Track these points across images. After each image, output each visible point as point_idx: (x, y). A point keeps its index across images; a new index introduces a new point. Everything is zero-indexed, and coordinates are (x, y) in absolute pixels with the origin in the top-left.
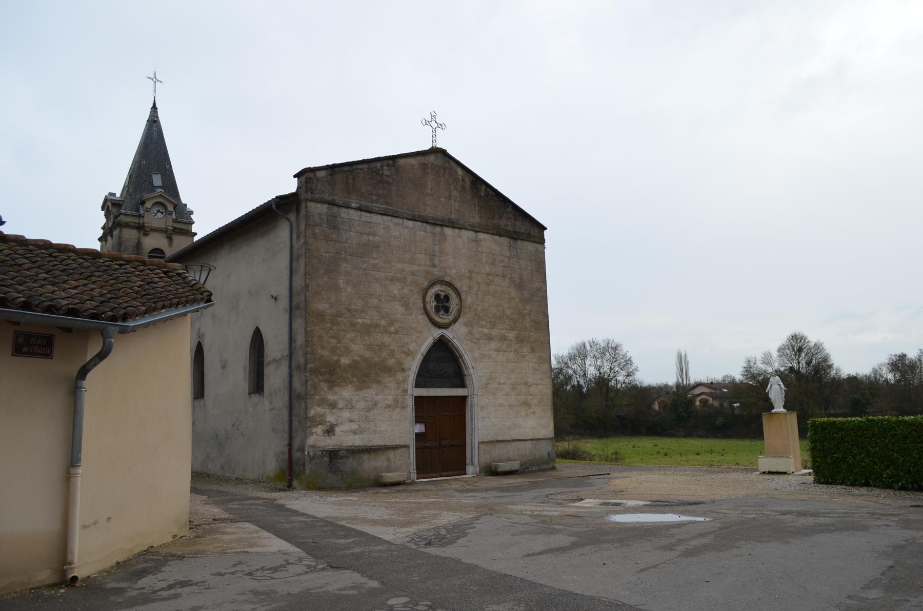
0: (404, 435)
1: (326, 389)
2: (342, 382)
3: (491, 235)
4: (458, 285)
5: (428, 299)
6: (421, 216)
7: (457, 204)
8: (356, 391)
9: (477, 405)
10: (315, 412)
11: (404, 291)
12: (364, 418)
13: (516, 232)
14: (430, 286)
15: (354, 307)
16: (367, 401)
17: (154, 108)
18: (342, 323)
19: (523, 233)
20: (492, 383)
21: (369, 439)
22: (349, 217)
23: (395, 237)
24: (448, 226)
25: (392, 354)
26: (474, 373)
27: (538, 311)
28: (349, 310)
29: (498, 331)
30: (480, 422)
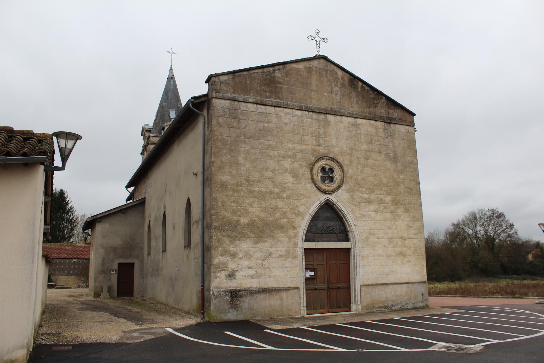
0: (295, 279)
1: (228, 242)
2: (241, 237)
3: (368, 121)
4: (340, 159)
5: (315, 171)
6: (307, 107)
7: (338, 97)
8: (254, 244)
9: (359, 255)
10: (219, 261)
12: (261, 266)
13: (390, 118)
14: (316, 161)
16: (263, 252)
17: (171, 70)
18: (242, 191)
19: (396, 118)
20: (371, 237)
21: (265, 282)
22: (247, 109)
23: (286, 124)
24: (331, 114)
25: (284, 215)
26: (356, 230)
28: (248, 181)
29: (376, 196)
30: (361, 269)
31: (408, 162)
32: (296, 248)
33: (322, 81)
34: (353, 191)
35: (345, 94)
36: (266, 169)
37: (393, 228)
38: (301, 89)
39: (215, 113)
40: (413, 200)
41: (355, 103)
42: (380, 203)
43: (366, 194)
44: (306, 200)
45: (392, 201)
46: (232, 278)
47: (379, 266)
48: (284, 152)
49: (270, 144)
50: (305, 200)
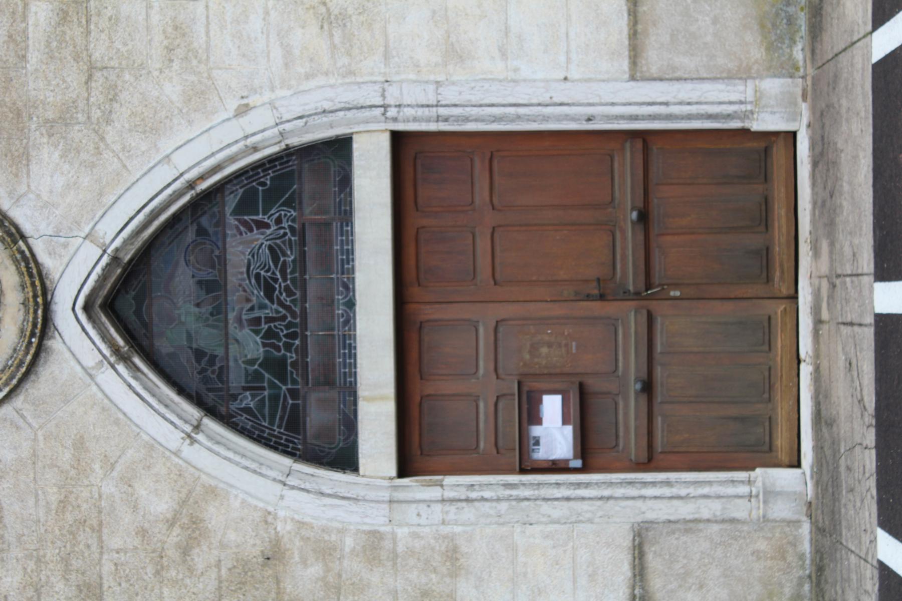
9: (438, 83)
26: (272, 105)
34: (19, 115)
44: (97, 466)
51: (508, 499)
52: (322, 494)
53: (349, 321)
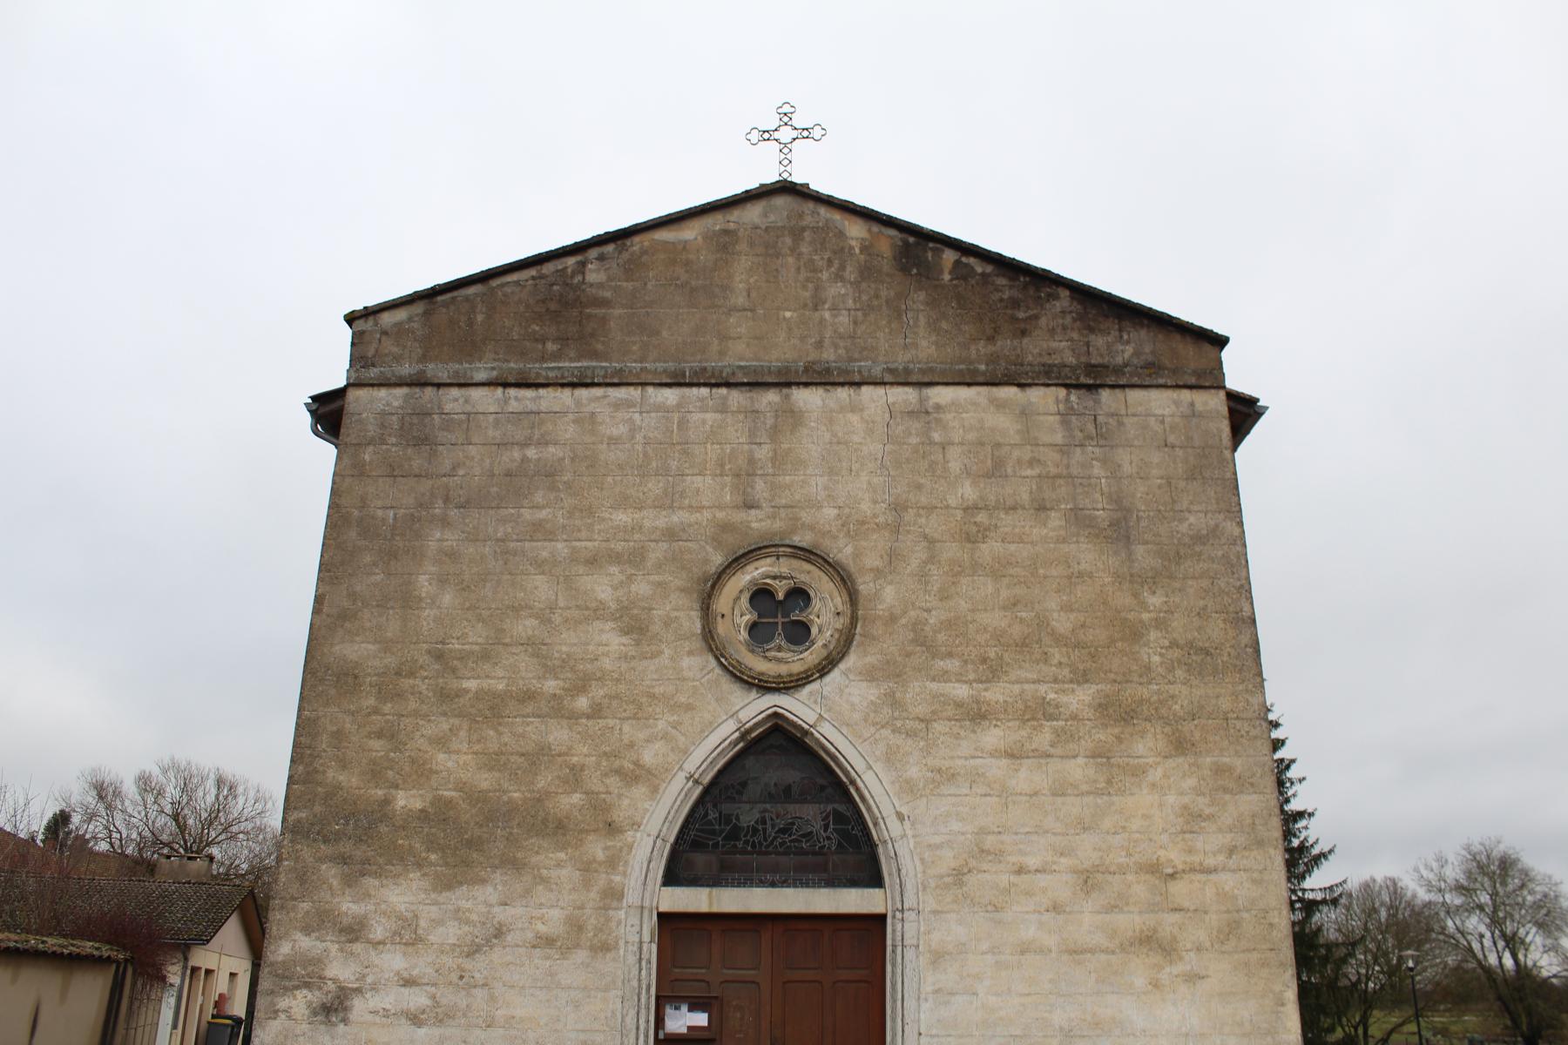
1: (335, 883)
4: (842, 551)
5: (722, 603)
6: (704, 369)
7: (844, 319)
8: (434, 890)
11: (634, 588)
12: (454, 977)
13: (1091, 369)
14: (729, 566)
15: (457, 646)
16: (468, 922)
18: (412, 694)
19: (1126, 365)
20: (985, 866)
22: (468, 408)
23: (613, 441)
24: (806, 385)
25: (574, 777)
26: (904, 836)
27: (1205, 608)
28: (439, 656)
29: (1016, 688)
30: (925, 1006)
31: (1192, 538)
32: (616, 909)
33: (777, 270)
34: (898, 676)
35: (875, 303)
36: (517, 609)
37: (1107, 823)
38: (685, 310)
39: (348, 435)
40: (1218, 697)
41: (922, 331)
42: (1033, 719)
43: (966, 682)
44: (675, 718)
45: (1100, 705)
46: (334, 1019)
47: (1021, 995)
48: (596, 544)
49: (541, 520)
50: (671, 719)
51: (640, 987)
52: (650, 862)
53: (762, 883)
